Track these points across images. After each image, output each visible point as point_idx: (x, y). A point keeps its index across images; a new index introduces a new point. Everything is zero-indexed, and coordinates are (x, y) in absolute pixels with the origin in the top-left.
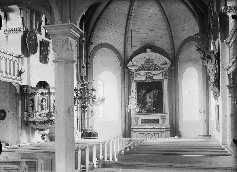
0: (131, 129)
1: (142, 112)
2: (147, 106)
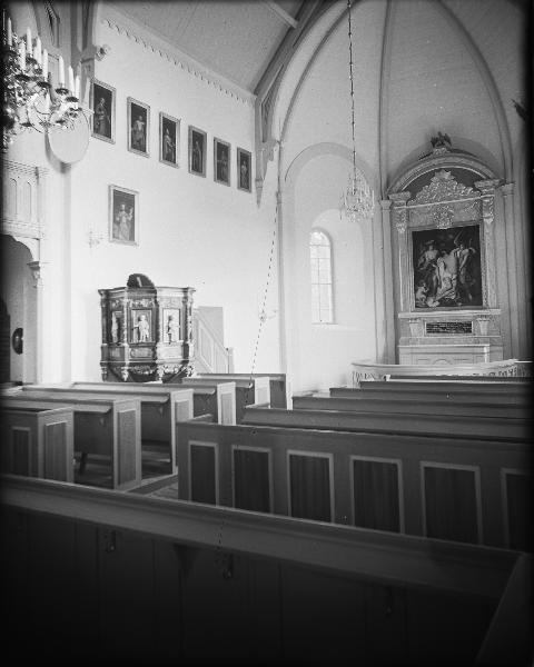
2: (440, 290)
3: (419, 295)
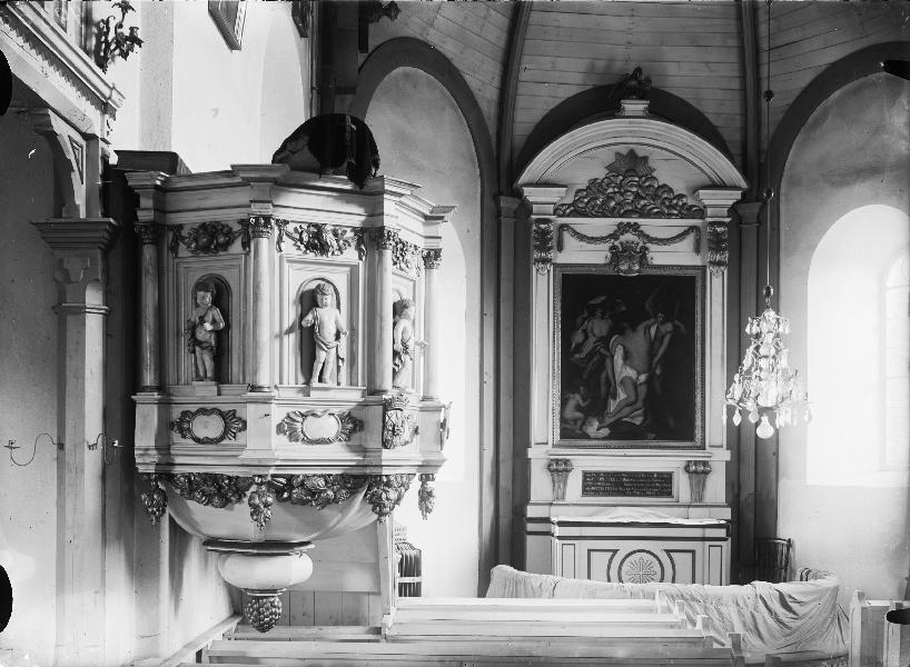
0: (530, 527)
1: (587, 437)
2: (613, 406)
3: (571, 413)
